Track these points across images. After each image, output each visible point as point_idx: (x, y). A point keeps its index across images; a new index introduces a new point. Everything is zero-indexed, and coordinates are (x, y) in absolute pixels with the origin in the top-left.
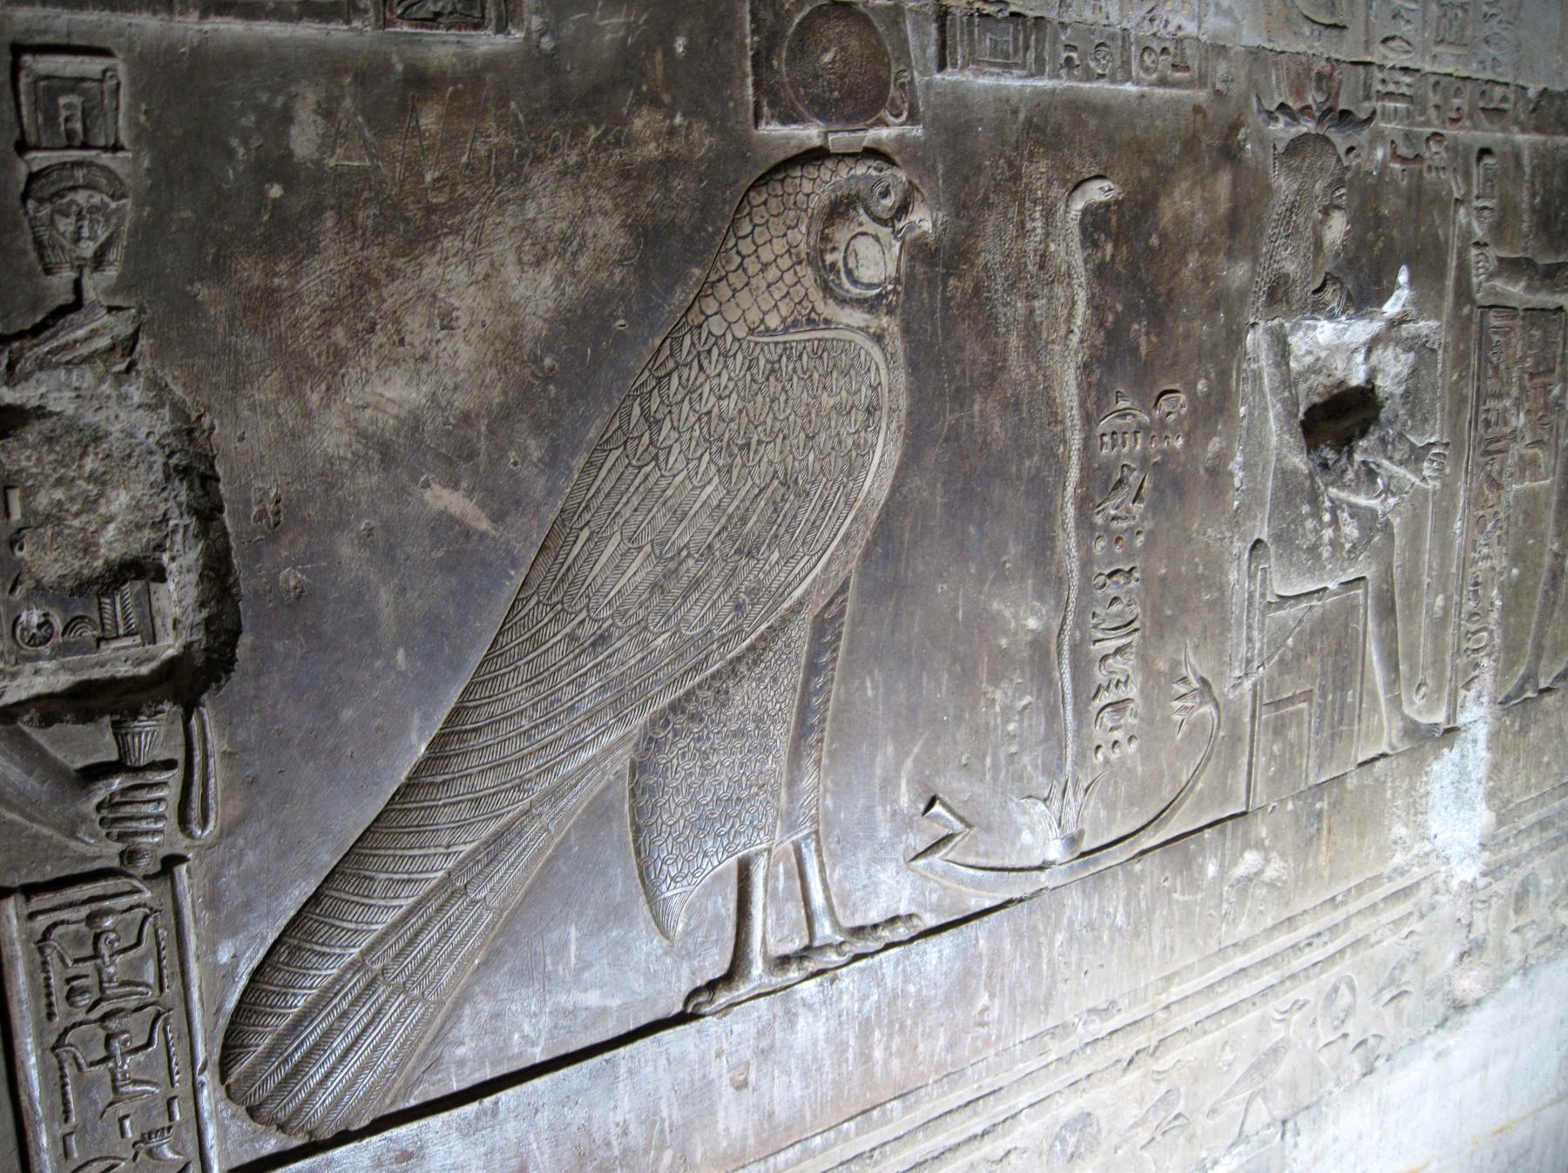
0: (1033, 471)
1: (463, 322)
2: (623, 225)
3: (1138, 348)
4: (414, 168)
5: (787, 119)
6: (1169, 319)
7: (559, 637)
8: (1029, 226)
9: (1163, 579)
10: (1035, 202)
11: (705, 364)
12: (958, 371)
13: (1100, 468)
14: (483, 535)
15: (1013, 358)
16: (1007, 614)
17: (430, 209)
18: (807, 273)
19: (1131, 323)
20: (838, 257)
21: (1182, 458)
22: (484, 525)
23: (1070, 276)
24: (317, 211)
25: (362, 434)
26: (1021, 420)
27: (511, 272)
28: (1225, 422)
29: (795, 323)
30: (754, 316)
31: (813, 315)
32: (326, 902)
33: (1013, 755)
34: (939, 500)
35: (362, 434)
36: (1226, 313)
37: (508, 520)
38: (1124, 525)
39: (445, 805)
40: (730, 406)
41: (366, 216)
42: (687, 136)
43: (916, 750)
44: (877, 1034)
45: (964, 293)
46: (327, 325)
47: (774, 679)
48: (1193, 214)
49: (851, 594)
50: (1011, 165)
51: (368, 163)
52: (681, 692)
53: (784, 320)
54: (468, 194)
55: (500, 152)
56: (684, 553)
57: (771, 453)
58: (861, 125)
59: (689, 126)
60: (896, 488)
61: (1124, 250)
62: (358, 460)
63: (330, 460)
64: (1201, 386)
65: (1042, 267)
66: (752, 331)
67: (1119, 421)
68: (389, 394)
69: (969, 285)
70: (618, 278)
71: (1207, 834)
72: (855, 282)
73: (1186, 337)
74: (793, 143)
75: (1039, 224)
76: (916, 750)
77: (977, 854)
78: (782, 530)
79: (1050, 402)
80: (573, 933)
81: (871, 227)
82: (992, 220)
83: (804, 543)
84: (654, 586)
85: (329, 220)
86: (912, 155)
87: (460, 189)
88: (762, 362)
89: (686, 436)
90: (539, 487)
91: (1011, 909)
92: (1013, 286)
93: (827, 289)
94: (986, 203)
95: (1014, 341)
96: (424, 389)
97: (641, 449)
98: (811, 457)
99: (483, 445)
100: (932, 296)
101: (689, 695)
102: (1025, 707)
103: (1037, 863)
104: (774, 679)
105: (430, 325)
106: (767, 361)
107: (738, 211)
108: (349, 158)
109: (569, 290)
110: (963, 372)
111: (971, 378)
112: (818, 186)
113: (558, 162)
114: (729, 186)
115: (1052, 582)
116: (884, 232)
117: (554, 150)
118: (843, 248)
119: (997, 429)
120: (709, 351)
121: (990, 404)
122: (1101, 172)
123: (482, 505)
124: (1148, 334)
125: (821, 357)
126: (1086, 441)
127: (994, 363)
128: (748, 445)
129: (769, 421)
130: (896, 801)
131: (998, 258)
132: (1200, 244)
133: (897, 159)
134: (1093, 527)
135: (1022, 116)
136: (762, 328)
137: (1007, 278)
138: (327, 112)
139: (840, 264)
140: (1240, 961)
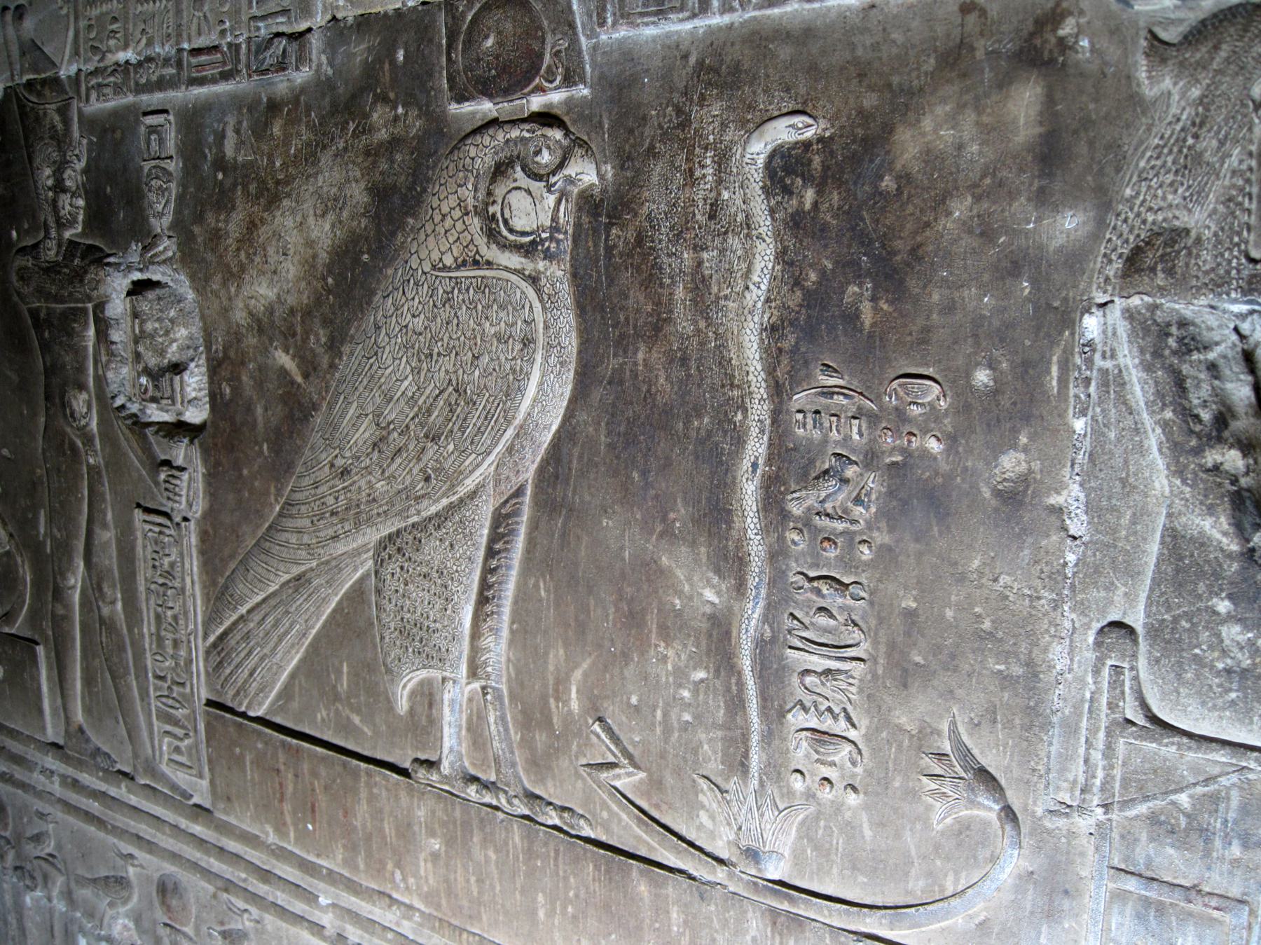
0: (703, 433)
1: (291, 252)
2: (366, 189)
3: (857, 316)
6: (913, 284)
8: (698, 174)
9: (910, 614)
10: (706, 149)
12: (622, 318)
13: (794, 449)
14: (299, 385)
15: (679, 311)
16: (680, 574)
17: (278, 182)
18: (475, 223)
19: (849, 283)
22: (299, 379)
23: (748, 227)
24: (235, 185)
25: (250, 313)
26: (689, 376)
27: (311, 220)
28: (1032, 438)
29: (464, 263)
30: (435, 255)
31: (477, 257)
34: (603, 438)
35: (250, 313)
36: (1034, 282)
38: (840, 526)
40: (419, 323)
41: (252, 188)
43: (585, 666)
45: (626, 243)
46: (238, 249)
48: (960, 147)
49: (527, 499)
50: (679, 111)
52: (394, 529)
53: (456, 260)
56: (392, 427)
57: (448, 363)
58: (518, 95)
59: (406, 114)
61: (835, 196)
62: (250, 327)
63: (238, 325)
65: (712, 216)
66: (434, 267)
67: (823, 400)
68: (261, 292)
69: (631, 235)
72: (511, 231)
73: (949, 308)
75: (710, 171)
76: (585, 666)
78: (456, 428)
79: (724, 363)
82: (658, 169)
83: (472, 443)
84: (375, 445)
88: (441, 291)
89: (393, 341)
90: (325, 361)
92: (679, 235)
93: (492, 235)
94: (652, 153)
95: (680, 292)
98: (477, 373)
99: (299, 329)
100: (596, 245)
101: (398, 532)
105: (278, 252)
106: (444, 292)
110: (627, 319)
111: (635, 327)
112: (483, 153)
114: (430, 155)
116: (537, 186)
117: (332, 140)
118: (500, 201)
119: (662, 381)
121: (655, 355)
122: (799, 107)
123: (298, 366)
124: (874, 299)
125: (483, 292)
126: (777, 415)
127: (659, 314)
128: (431, 355)
129: (446, 340)
131: (663, 207)
132: (975, 186)
133: (566, 119)
134: (785, 515)
137: (672, 228)
139: (499, 215)
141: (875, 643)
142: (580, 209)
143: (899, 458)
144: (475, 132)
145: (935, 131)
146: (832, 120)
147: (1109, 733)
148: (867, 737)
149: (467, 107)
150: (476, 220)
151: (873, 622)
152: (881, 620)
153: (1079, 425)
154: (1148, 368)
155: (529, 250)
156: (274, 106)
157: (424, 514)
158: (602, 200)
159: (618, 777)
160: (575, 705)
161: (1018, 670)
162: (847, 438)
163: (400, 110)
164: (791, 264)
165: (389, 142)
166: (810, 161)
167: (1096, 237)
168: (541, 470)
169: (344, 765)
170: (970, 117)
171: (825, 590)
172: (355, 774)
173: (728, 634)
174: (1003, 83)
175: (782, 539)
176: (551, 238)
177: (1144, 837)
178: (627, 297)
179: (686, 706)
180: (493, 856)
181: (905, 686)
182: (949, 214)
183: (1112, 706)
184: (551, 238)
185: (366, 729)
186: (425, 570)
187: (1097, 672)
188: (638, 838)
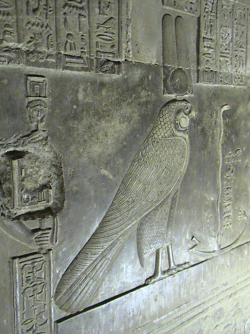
7: (125, 201)
8: (213, 115)
10: (214, 110)
11: (153, 144)
24: (83, 111)
29: (170, 136)
32: (78, 259)
33: (208, 227)
37: (116, 176)
39: (102, 237)
42: (151, 96)
44: (182, 288)
47: (165, 210)
49: (179, 192)
50: (210, 102)
51: (92, 101)
54: (111, 108)
55: (117, 99)
60: (188, 170)
69: (202, 128)
70: (138, 126)
72: (181, 127)
74: (170, 98)
75: (215, 115)
81: (185, 116)
85: (85, 112)
86: (191, 100)
87: (109, 107)
89: (150, 159)
91: (208, 261)
93: (176, 128)
96: (102, 149)
97: (141, 162)
100: (195, 130)
102: (211, 217)
103: (212, 251)
104: (165, 210)
107: (160, 112)
108: (89, 100)
109: (129, 128)
112: (174, 106)
116: (187, 117)
120: (154, 141)
126: (223, 160)
135: (212, 92)
136: (164, 137)
138: (85, 90)
139: (179, 124)
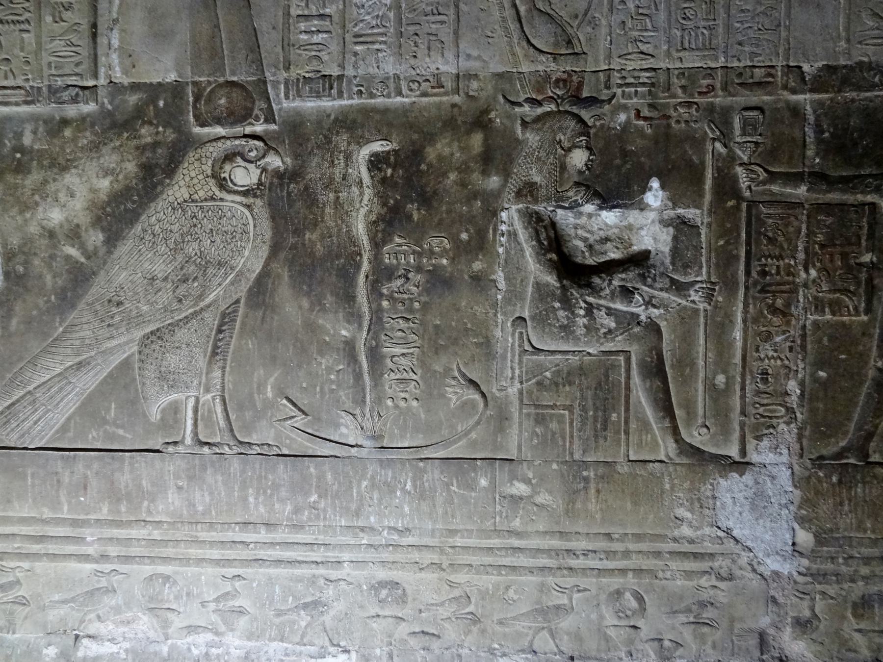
0: (340, 266)
1: (78, 194)
3: (412, 215)
4: (62, 148)
5: (202, 125)
6: (435, 204)
8: (336, 162)
9: (436, 327)
13: (385, 268)
14: (82, 263)
15: (327, 218)
16: (328, 326)
18: (212, 182)
20: (226, 175)
21: (449, 269)
22: (83, 260)
28: (484, 256)
36: (482, 203)
38: (406, 296)
43: (276, 375)
44: (250, 491)
45: (299, 190)
48: (452, 154)
50: (326, 137)
52: (155, 328)
55: (92, 142)
59: (165, 132)
61: (401, 172)
64: (464, 236)
65: (344, 179)
69: (301, 186)
71: (479, 463)
76: (276, 375)
77: (313, 429)
80: (113, 406)
81: (242, 163)
82: (315, 161)
88: (190, 213)
92: (327, 187)
101: (158, 330)
103: (353, 443)
109: (115, 186)
110: (299, 222)
113: (112, 145)
115: (354, 317)
116: (251, 167)
123: (82, 254)
124: (418, 209)
130: (265, 394)
131: (318, 176)
133: (265, 138)
134: (381, 295)
135: (332, 117)
140: (516, 542)
141: (423, 339)
142: (273, 176)
143: (431, 268)
144: (210, 141)
145: (442, 148)
146: (399, 143)
147: (520, 356)
148: (422, 377)
149: (206, 130)
150: (213, 180)
151: (421, 332)
152: (425, 331)
153: (501, 250)
154: (526, 228)
155: (245, 194)
156: (65, 122)
157: (176, 318)
158: (285, 173)
159: (296, 422)
160: (270, 394)
161: (482, 340)
162: (408, 263)
163: (161, 129)
164: (381, 197)
165: (153, 144)
166: (389, 158)
167: (504, 186)
168: (250, 290)
169: (113, 458)
170: (456, 144)
171: (401, 321)
172: (122, 460)
173: (354, 348)
174: (469, 133)
175: (380, 305)
176: (258, 188)
177: (535, 390)
178: (299, 213)
179: (332, 382)
180: (220, 478)
181: (436, 353)
182: (448, 178)
183: (520, 346)
184: (258, 188)
185: (128, 435)
186: (177, 345)
187: (513, 335)
188: (307, 447)
